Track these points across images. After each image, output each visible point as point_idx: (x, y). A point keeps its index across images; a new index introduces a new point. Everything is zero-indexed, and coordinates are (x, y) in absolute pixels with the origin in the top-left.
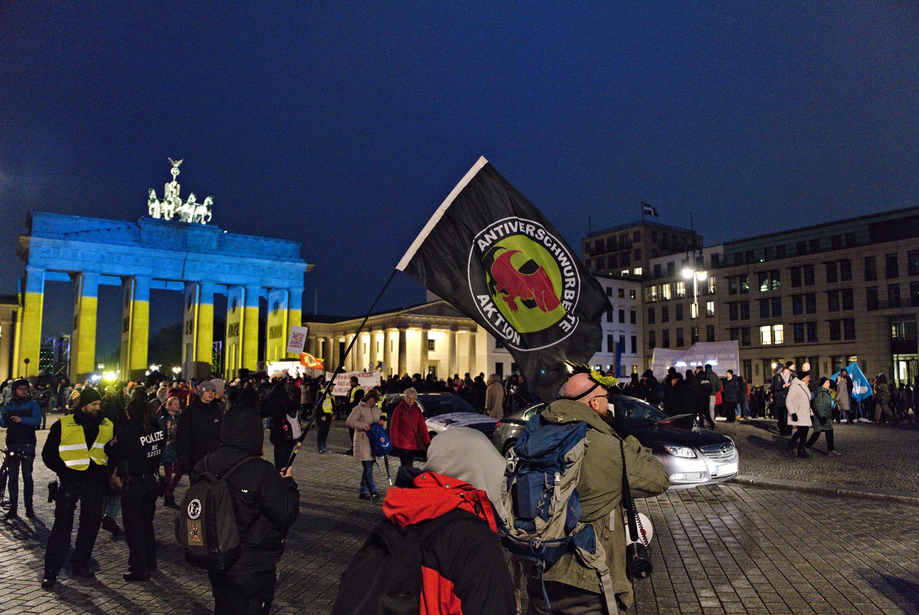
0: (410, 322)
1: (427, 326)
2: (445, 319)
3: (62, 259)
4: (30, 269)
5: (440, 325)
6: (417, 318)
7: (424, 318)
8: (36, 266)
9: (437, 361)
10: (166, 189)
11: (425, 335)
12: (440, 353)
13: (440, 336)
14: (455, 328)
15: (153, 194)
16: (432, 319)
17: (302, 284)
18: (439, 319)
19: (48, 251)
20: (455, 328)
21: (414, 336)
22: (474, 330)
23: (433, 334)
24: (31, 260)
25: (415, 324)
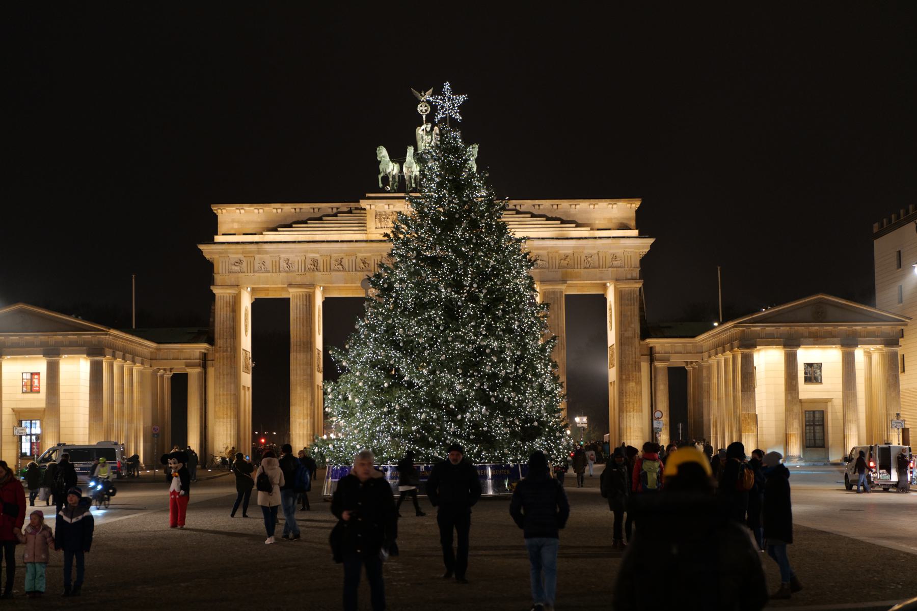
0: (758, 336)
1: (791, 343)
2: (828, 328)
3: (257, 272)
4: (216, 291)
5: (819, 340)
6: (770, 329)
7: (784, 329)
8: (224, 286)
9: (826, 402)
10: (418, 137)
11: (791, 361)
12: (830, 386)
13: (828, 357)
14: (849, 343)
15: (383, 153)
16: (800, 328)
17: (636, 273)
18: (815, 328)
19: (240, 262)
20: (849, 343)
21: (768, 360)
22: (892, 341)
23: (806, 355)
24: (218, 278)
25: (769, 341)
